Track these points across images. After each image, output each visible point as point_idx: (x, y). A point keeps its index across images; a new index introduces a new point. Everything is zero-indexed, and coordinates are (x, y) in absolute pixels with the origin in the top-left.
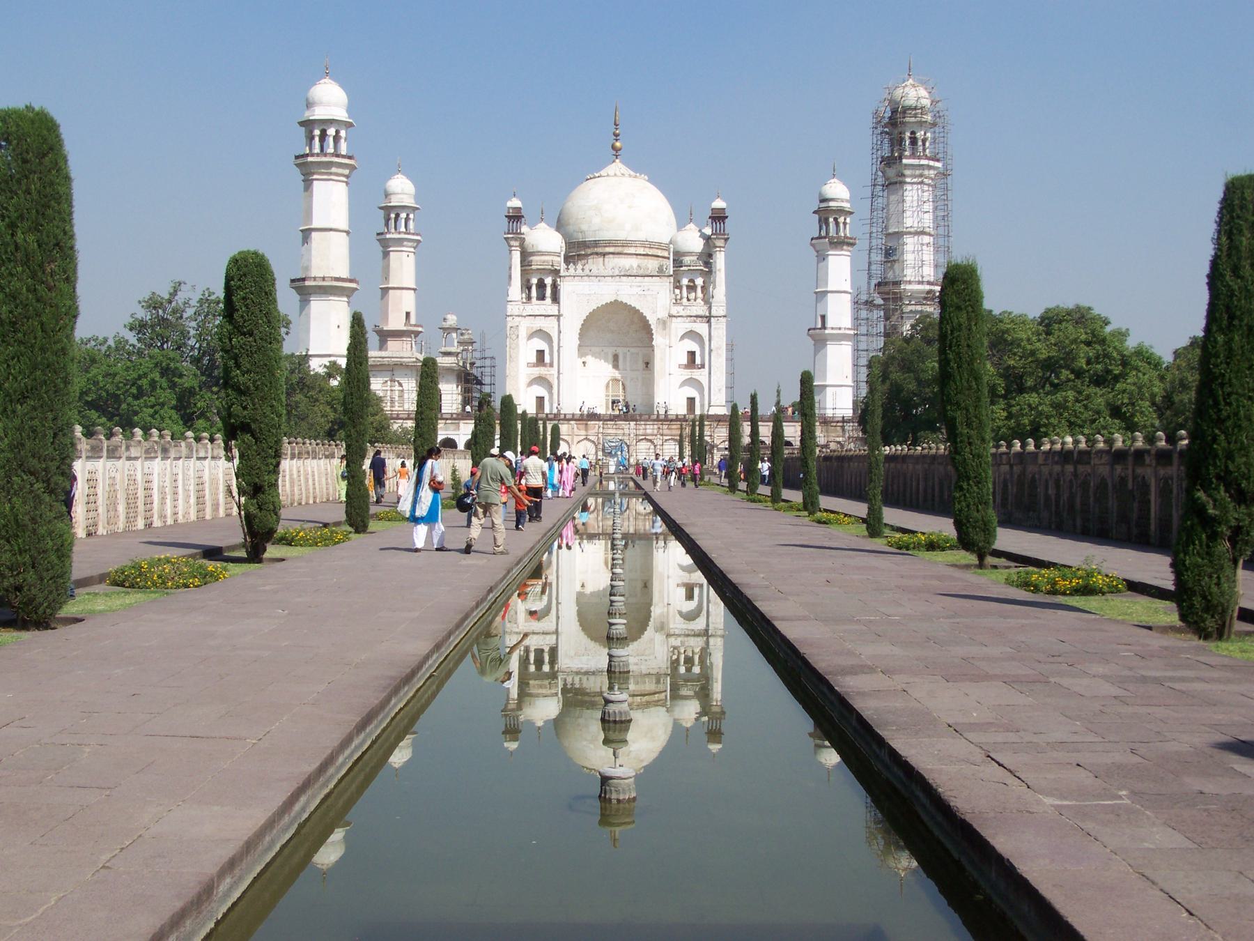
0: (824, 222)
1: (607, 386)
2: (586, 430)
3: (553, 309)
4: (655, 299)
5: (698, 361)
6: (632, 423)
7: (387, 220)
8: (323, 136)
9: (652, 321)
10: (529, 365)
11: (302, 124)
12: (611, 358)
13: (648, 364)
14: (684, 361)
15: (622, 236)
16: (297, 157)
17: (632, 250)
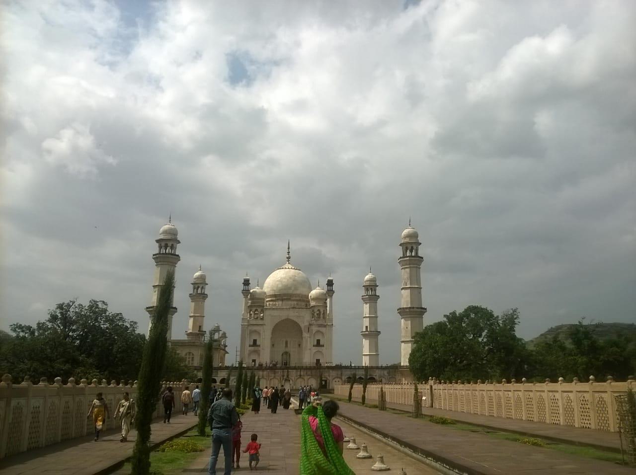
0: (367, 290)
1: (283, 354)
2: (275, 374)
3: (260, 322)
4: (304, 318)
5: (321, 343)
6: (295, 370)
7: (194, 288)
8: (166, 246)
9: (302, 326)
10: (250, 346)
11: (157, 241)
12: (284, 343)
13: (299, 345)
14: (315, 343)
15: (290, 292)
16: (154, 255)
17: (294, 298)
